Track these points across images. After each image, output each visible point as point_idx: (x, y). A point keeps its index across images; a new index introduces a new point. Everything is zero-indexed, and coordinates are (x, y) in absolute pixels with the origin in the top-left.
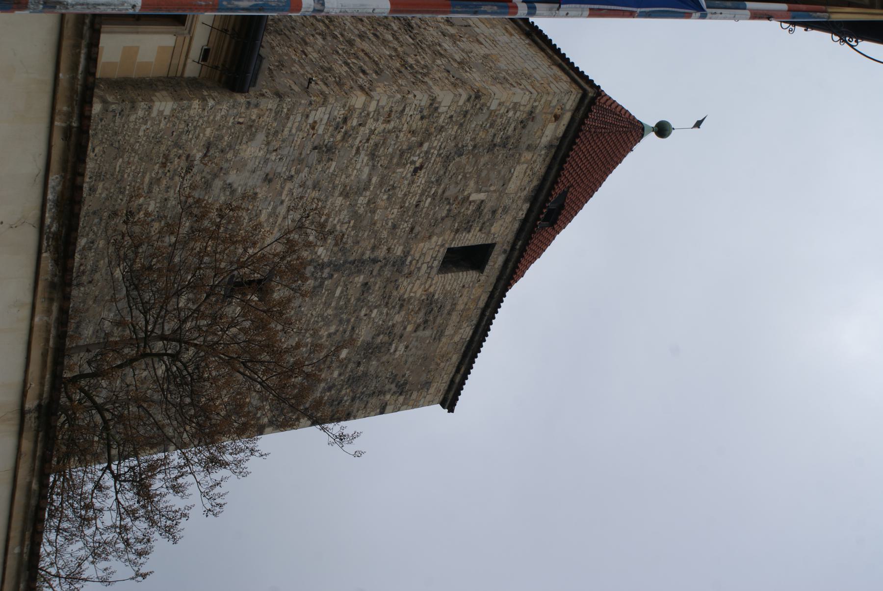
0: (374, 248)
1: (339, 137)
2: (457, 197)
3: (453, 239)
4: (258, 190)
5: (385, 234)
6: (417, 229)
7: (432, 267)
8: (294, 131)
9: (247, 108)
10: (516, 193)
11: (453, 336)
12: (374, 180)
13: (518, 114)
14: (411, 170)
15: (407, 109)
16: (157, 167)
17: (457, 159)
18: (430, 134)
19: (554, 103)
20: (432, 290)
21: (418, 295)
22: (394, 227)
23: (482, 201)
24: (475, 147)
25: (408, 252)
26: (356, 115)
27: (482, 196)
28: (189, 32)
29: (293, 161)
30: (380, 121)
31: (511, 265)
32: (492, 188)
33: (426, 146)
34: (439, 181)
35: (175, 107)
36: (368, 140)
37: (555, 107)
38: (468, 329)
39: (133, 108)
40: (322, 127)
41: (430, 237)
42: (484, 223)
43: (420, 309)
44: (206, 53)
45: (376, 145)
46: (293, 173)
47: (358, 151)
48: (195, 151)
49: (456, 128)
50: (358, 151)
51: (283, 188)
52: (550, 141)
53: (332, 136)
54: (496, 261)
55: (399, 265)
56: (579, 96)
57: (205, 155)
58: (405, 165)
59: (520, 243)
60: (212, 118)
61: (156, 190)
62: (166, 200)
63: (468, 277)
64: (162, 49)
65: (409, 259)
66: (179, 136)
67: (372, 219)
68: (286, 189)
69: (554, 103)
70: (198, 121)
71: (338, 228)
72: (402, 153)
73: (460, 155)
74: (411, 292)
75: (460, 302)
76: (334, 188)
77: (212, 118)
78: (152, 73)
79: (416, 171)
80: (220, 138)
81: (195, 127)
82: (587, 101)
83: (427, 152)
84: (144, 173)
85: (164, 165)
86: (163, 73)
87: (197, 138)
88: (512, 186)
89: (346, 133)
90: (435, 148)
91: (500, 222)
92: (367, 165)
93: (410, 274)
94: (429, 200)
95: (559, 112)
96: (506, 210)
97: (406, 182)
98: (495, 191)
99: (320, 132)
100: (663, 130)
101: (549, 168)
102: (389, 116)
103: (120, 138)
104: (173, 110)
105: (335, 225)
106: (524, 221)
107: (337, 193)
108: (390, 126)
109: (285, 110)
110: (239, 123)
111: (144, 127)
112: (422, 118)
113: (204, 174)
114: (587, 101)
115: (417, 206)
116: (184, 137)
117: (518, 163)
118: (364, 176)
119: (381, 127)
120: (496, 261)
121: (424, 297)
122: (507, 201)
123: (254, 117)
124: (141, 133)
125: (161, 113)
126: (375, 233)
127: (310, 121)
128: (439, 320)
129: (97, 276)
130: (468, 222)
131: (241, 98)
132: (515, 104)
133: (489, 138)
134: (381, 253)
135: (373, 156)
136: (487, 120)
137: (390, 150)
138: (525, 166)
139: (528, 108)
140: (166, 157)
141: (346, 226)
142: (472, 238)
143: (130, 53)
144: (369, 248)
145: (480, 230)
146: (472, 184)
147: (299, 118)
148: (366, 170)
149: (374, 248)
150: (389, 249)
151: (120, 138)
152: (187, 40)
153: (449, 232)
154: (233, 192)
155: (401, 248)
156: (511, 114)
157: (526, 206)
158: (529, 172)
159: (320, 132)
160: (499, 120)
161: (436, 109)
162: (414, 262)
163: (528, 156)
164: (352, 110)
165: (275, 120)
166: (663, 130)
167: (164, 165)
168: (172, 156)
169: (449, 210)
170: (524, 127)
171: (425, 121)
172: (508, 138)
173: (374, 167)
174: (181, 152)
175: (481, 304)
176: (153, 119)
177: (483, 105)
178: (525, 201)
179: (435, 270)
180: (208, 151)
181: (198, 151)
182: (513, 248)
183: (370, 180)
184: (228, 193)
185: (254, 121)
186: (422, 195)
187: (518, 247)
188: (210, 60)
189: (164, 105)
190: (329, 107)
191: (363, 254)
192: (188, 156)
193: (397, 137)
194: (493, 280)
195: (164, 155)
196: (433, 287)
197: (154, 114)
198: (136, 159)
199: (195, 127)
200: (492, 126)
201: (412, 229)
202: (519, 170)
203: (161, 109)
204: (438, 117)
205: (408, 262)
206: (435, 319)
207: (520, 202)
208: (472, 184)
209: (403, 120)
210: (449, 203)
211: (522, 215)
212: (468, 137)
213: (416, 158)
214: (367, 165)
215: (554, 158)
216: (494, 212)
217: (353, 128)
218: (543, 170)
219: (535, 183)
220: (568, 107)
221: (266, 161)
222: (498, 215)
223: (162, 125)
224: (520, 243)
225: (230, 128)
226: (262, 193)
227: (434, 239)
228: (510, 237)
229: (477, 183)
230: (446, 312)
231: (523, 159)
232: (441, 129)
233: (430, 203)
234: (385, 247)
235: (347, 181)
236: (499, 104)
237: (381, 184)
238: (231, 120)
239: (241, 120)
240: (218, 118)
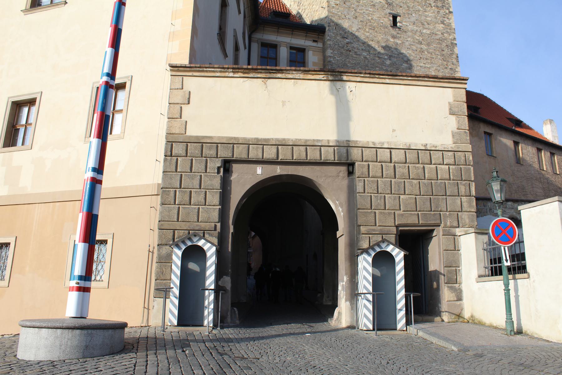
4: (360, 21)
8: (338, 11)
9: (330, 26)
16: (351, 53)
28: (308, 47)
29: (349, 10)
35: (330, 49)
39: (330, 62)
40: (337, 2)
44: (314, 41)
46: (354, 10)
48: (345, 42)
51: (359, 12)
57: (347, 38)
60: (333, 37)
61: (358, 53)
62: (362, 50)
64: (313, 55)
66: (339, 46)
68: (359, 11)
70: (335, 41)
77: (333, 37)
78: (321, 57)
80: (341, 34)
81: (337, 42)
84: (353, 57)
85: (350, 51)
86: (321, 53)
87: (340, 41)
103: (340, 65)
104: (331, 49)
109: (331, 14)
110: (335, 29)
111: (337, 58)
113: (353, 38)
116: (340, 45)
123: (334, 24)
124: (339, 59)
125: (332, 53)
127: (335, 6)
129: (389, 70)
131: (327, 29)
140: (347, 51)
147: (334, 10)
151: (340, 65)
152: (310, 47)
154: (360, 28)
159: (339, 2)
165: (334, 17)
167: (350, 51)
168: (347, 49)
174: (345, 46)
176: (334, 55)
180: (345, 38)
181: (345, 40)
184: (360, 30)
185: (335, 24)
188: (317, 40)
189: (329, 52)
192: (347, 44)
195: (346, 51)
197: (332, 55)
198: (348, 60)
199: (337, 42)
203: (330, 53)
221: (349, 19)
223: (336, 52)
225: (337, 31)
226: (360, 19)
238: (335, 31)
239: (334, 28)
240: (334, 35)
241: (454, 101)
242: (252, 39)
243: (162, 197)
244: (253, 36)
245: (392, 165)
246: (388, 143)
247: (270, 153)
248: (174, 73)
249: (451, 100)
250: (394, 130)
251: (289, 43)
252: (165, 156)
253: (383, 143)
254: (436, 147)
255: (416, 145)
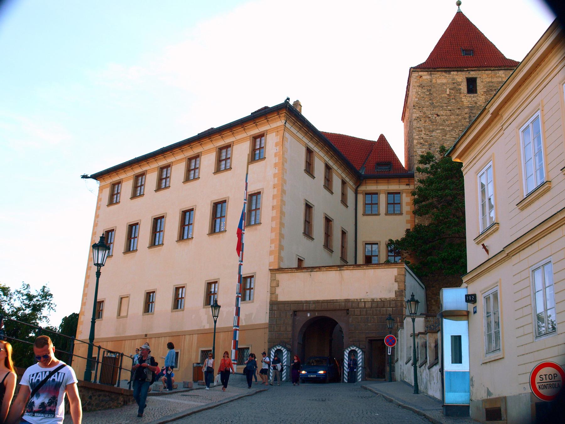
0: (465, 119)
1: (426, 143)
2: (448, 98)
3: (463, 93)
5: (460, 117)
6: (459, 107)
7: (474, 96)
10: (447, 78)
11: (502, 77)
12: (441, 128)
13: (419, 90)
14: (438, 117)
15: (418, 126)
17: (435, 104)
18: (426, 116)
19: (416, 80)
20: (482, 93)
21: (484, 97)
22: (458, 115)
23: (450, 89)
24: (430, 100)
25: (467, 107)
26: (419, 141)
27: (448, 90)
30: (421, 133)
31: (474, 69)
32: (445, 88)
33: (430, 116)
34: (442, 107)
36: (428, 134)
37: (417, 79)
38: (500, 73)
41: (462, 102)
42: (458, 85)
43: (490, 94)
44: (407, 185)
45: (429, 131)
47: (431, 136)
49: (424, 109)
50: (431, 136)
52: (429, 75)
53: (426, 146)
54: (473, 74)
55: (471, 108)
56: (413, 73)
58: (436, 120)
59: (465, 70)
63: (478, 81)
64: (407, 196)
65: (470, 105)
67: (455, 123)
69: (416, 80)
71: (457, 133)
72: (432, 122)
73: (433, 103)
74: (483, 100)
75: (488, 80)
76: (443, 139)
79: (438, 115)
82: (414, 70)
83: (432, 115)
88: (444, 81)
89: (425, 142)
90: (430, 113)
91: (458, 79)
92: (436, 132)
93: (476, 103)
94: (448, 107)
95: (419, 77)
96: (453, 79)
97: (442, 117)
98: (446, 87)
99: (424, 150)
100: (459, 4)
101: (438, 71)
102: (420, 131)
105: (457, 134)
106: (457, 71)
107: (445, 138)
108: (423, 129)
112: (421, 121)
114: (414, 70)
115: (450, 110)
117: (436, 83)
118: (440, 131)
119: (423, 132)
120: (473, 74)
121: (485, 95)
122: (450, 81)
126: (459, 120)
128: (495, 85)
130: (457, 91)
132: (416, 93)
133: (428, 96)
134: (467, 116)
135: (433, 131)
136: (421, 100)
137: (431, 126)
138: (437, 80)
139: (417, 88)
141: (457, 131)
142: (464, 87)
143: (407, 204)
144: (465, 120)
145: (460, 85)
146: (443, 95)
148: (438, 131)
149: (465, 119)
150: (466, 114)
153: (461, 96)
155: (466, 110)
156: (419, 93)
157: (452, 73)
158: (440, 78)
160: (422, 96)
161: (418, 117)
162: (471, 103)
163: (434, 81)
164: (418, 143)
166: (459, 4)
169: (453, 99)
170: (424, 86)
171: (422, 119)
172: (428, 90)
173: (437, 129)
175: (490, 72)
177: (416, 103)
178: (450, 74)
179: (476, 95)
182: (468, 71)
183: (441, 129)
186: (447, 110)
187: (467, 70)
188: (408, 183)
190: (417, 150)
191: (467, 122)
193: (427, 126)
194: (480, 72)
196: (481, 93)
200: (423, 97)
201: (459, 109)
202: (439, 81)
204: (420, 116)
205: (471, 105)
206: (494, 87)
207: (450, 76)
208: (443, 95)
209: (421, 126)
210: (450, 100)
211: (455, 73)
212: (427, 103)
213: (434, 117)
214: (436, 132)
215: (434, 71)
216: (454, 83)
217: (424, 140)
218: (439, 73)
219: (444, 74)
220: (417, 75)
222: (455, 81)
224: (465, 70)
225: (423, 176)
227: (463, 100)
228: (463, 73)
229: (443, 94)
230: (492, 84)
231: (435, 82)
232: (425, 113)
233: (450, 106)
234: (465, 115)
235: (441, 136)
236: (416, 98)
237: (442, 125)
241: (398, 275)
242: (358, 191)
243: (269, 329)
244: (358, 189)
245: (365, 309)
246: (363, 299)
247: (312, 307)
248: (272, 273)
249: (396, 274)
250: (367, 293)
251: (386, 190)
252: (270, 310)
253: (361, 300)
254: (386, 299)
255: (377, 299)
